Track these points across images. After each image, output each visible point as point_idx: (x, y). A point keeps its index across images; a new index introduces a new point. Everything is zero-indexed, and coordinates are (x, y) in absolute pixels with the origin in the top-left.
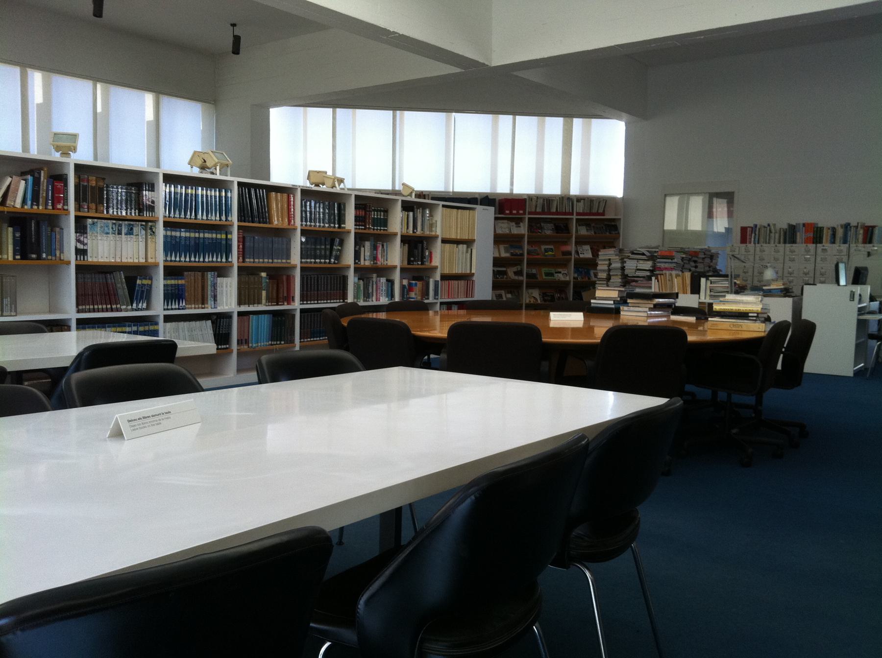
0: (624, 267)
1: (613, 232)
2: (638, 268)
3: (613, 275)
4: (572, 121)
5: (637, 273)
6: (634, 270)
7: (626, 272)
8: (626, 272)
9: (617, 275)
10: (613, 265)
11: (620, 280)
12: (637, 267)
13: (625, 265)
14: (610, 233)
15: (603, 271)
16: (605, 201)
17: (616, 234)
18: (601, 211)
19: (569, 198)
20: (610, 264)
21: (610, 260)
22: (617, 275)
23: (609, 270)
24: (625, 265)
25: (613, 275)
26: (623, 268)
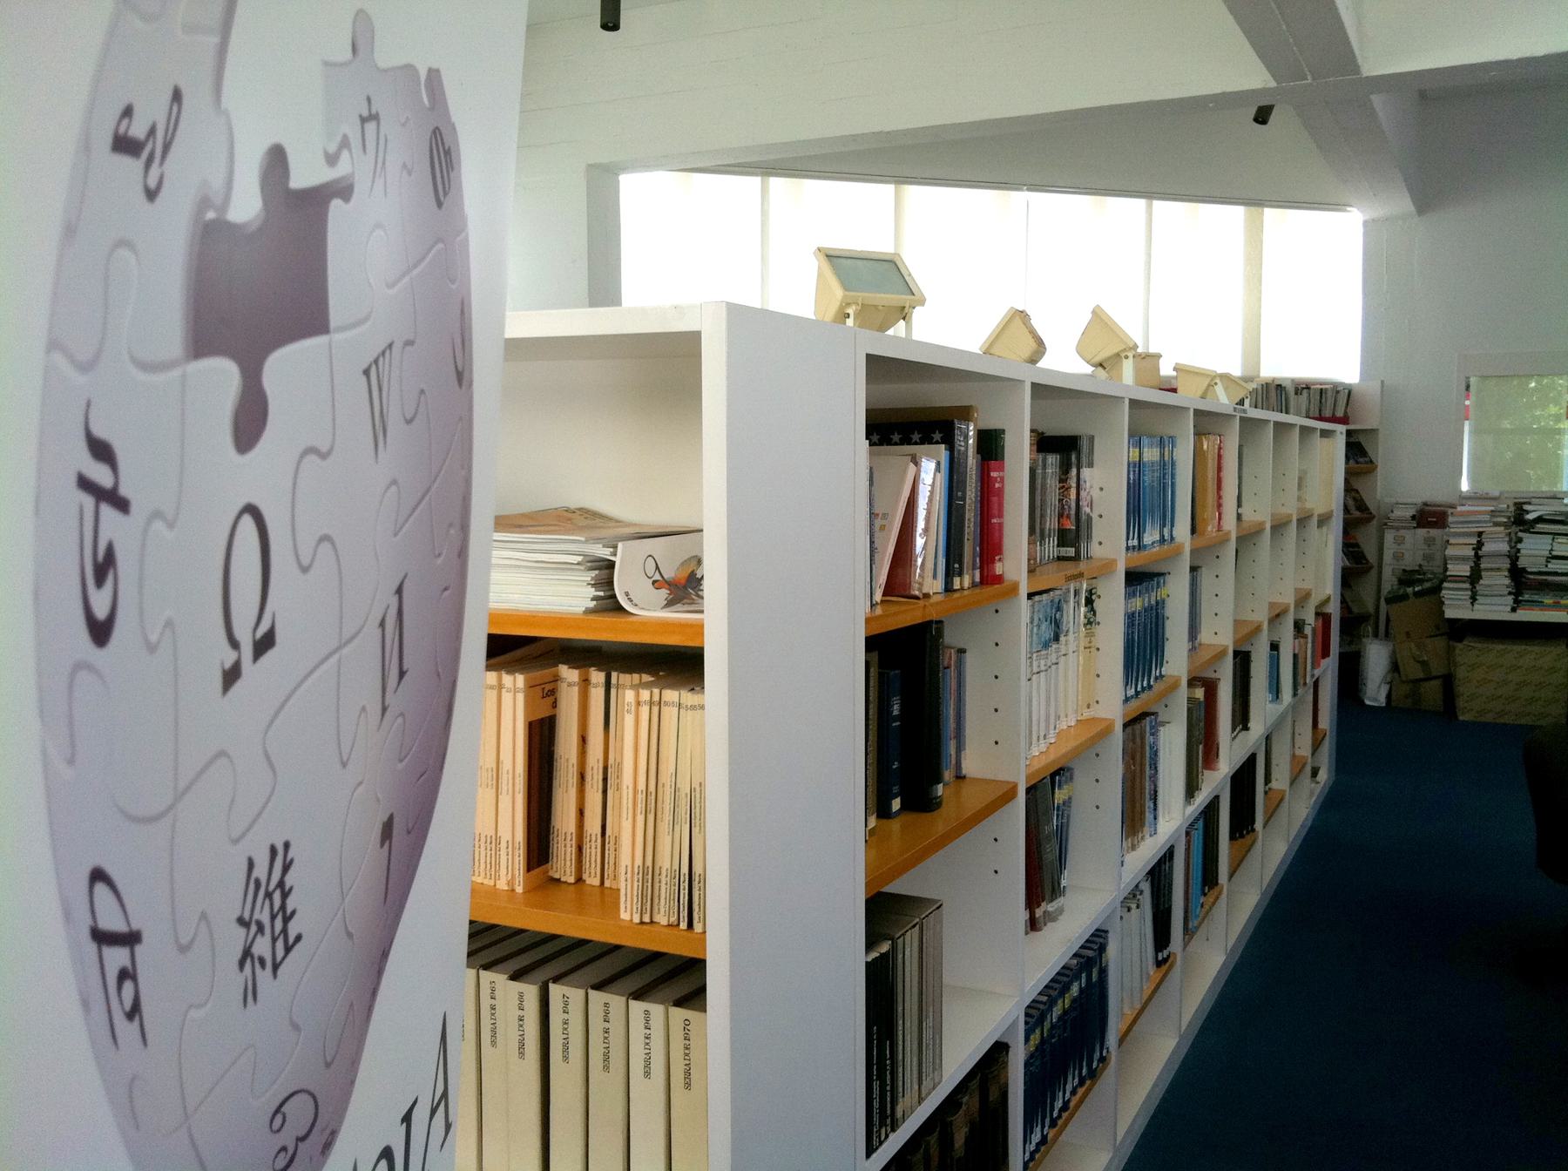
0: (1519, 550)
1: (1361, 460)
2: (1554, 553)
3: (1487, 570)
4: (1262, 214)
5: (1549, 565)
6: (1543, 560)
7: (1522, 563)
8: (1522, 563)
9: (1499, 569)
10: (1488, 547)
11: (1507, 581)
12: (1552, 550)
13: (1519, 546)
14: (1357, 463)
15: (1464, 559)
16: (1347, 391)
17: (1366, 463)
18: (1340, 413)
19: (1280, 386)
20: (1480, 545)
21: (1480, 534)
22: (1499, 569)
23: (1478, 557)
24: (1519, 546)
25: (1487, 570)
26: (1514, 557)
